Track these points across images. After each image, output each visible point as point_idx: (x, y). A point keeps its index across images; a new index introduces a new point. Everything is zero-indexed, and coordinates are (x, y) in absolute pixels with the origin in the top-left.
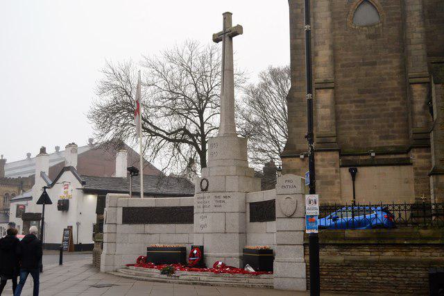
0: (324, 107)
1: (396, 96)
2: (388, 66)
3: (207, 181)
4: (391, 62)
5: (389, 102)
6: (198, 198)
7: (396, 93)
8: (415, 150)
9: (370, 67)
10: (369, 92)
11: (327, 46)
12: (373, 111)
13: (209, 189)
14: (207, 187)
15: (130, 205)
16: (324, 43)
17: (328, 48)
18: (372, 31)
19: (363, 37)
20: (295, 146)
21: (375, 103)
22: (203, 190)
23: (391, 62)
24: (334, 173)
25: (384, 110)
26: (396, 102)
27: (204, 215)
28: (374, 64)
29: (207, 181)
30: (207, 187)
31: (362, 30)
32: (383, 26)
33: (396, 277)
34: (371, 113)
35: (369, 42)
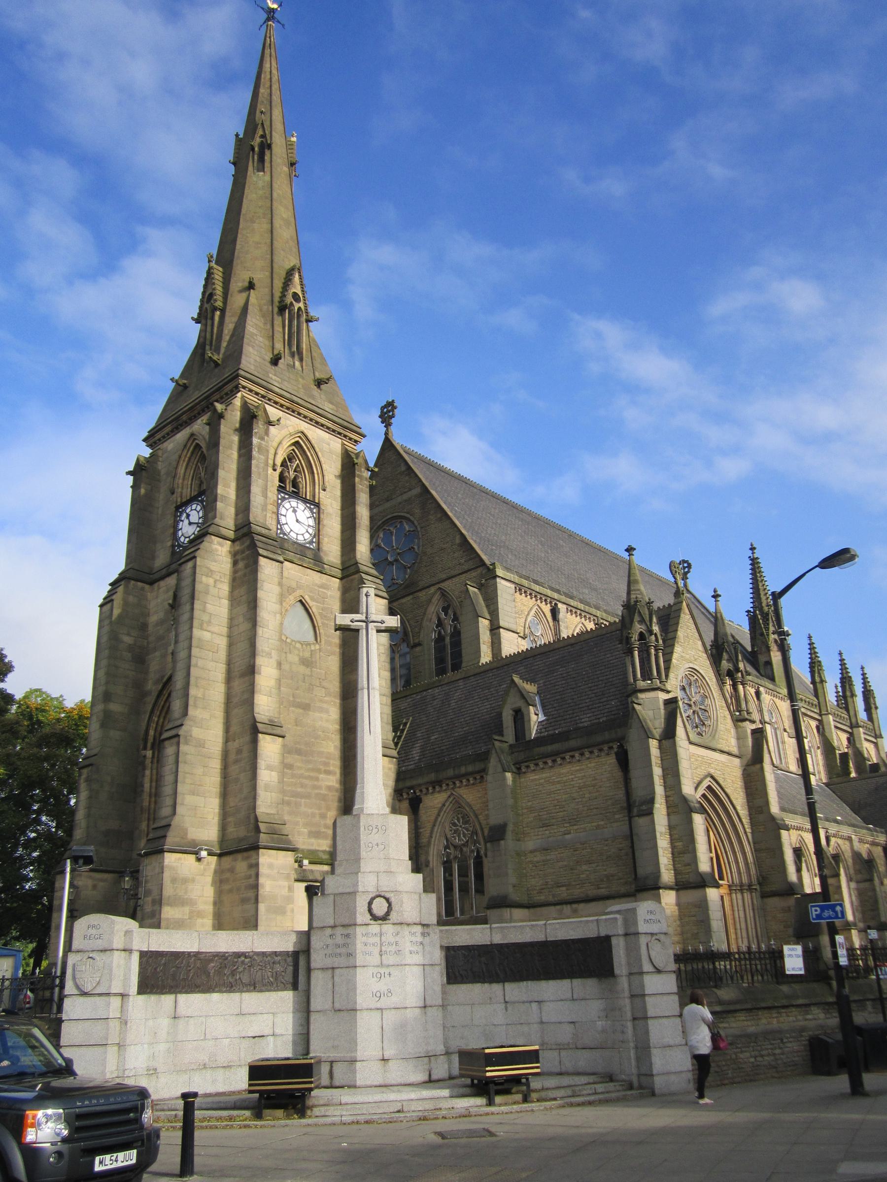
0: (269, 768)
1: (331, 768)
2: (324, 716)
3: (387, 900)
4: (327, 712)
5: (322, 776)
6: (366, 934)
7: (332, 762)
9: (301, 711)
10: (299, 752)
11: (273, 662)
12: (302, 785)
13: (393, 916)
14: (388, 913)
15: (154, 948)
16: (269, 655)
17: (275, 666)
18: (307, 654)
19: (296, 659)
20: (187, 830)
21: (307, 774)
22: (375, 918)
23: (327, 712)
24: (285, 892)
25: (315, 787)
26: (331, 777)
27: (382, 971)
28: (306, 707)
29: (387, 900)
30: (388, 913)
31: (295, 647)
32: (320, 650)
33: (774, 1054)
34: (299, 790)
35: (302, 669)
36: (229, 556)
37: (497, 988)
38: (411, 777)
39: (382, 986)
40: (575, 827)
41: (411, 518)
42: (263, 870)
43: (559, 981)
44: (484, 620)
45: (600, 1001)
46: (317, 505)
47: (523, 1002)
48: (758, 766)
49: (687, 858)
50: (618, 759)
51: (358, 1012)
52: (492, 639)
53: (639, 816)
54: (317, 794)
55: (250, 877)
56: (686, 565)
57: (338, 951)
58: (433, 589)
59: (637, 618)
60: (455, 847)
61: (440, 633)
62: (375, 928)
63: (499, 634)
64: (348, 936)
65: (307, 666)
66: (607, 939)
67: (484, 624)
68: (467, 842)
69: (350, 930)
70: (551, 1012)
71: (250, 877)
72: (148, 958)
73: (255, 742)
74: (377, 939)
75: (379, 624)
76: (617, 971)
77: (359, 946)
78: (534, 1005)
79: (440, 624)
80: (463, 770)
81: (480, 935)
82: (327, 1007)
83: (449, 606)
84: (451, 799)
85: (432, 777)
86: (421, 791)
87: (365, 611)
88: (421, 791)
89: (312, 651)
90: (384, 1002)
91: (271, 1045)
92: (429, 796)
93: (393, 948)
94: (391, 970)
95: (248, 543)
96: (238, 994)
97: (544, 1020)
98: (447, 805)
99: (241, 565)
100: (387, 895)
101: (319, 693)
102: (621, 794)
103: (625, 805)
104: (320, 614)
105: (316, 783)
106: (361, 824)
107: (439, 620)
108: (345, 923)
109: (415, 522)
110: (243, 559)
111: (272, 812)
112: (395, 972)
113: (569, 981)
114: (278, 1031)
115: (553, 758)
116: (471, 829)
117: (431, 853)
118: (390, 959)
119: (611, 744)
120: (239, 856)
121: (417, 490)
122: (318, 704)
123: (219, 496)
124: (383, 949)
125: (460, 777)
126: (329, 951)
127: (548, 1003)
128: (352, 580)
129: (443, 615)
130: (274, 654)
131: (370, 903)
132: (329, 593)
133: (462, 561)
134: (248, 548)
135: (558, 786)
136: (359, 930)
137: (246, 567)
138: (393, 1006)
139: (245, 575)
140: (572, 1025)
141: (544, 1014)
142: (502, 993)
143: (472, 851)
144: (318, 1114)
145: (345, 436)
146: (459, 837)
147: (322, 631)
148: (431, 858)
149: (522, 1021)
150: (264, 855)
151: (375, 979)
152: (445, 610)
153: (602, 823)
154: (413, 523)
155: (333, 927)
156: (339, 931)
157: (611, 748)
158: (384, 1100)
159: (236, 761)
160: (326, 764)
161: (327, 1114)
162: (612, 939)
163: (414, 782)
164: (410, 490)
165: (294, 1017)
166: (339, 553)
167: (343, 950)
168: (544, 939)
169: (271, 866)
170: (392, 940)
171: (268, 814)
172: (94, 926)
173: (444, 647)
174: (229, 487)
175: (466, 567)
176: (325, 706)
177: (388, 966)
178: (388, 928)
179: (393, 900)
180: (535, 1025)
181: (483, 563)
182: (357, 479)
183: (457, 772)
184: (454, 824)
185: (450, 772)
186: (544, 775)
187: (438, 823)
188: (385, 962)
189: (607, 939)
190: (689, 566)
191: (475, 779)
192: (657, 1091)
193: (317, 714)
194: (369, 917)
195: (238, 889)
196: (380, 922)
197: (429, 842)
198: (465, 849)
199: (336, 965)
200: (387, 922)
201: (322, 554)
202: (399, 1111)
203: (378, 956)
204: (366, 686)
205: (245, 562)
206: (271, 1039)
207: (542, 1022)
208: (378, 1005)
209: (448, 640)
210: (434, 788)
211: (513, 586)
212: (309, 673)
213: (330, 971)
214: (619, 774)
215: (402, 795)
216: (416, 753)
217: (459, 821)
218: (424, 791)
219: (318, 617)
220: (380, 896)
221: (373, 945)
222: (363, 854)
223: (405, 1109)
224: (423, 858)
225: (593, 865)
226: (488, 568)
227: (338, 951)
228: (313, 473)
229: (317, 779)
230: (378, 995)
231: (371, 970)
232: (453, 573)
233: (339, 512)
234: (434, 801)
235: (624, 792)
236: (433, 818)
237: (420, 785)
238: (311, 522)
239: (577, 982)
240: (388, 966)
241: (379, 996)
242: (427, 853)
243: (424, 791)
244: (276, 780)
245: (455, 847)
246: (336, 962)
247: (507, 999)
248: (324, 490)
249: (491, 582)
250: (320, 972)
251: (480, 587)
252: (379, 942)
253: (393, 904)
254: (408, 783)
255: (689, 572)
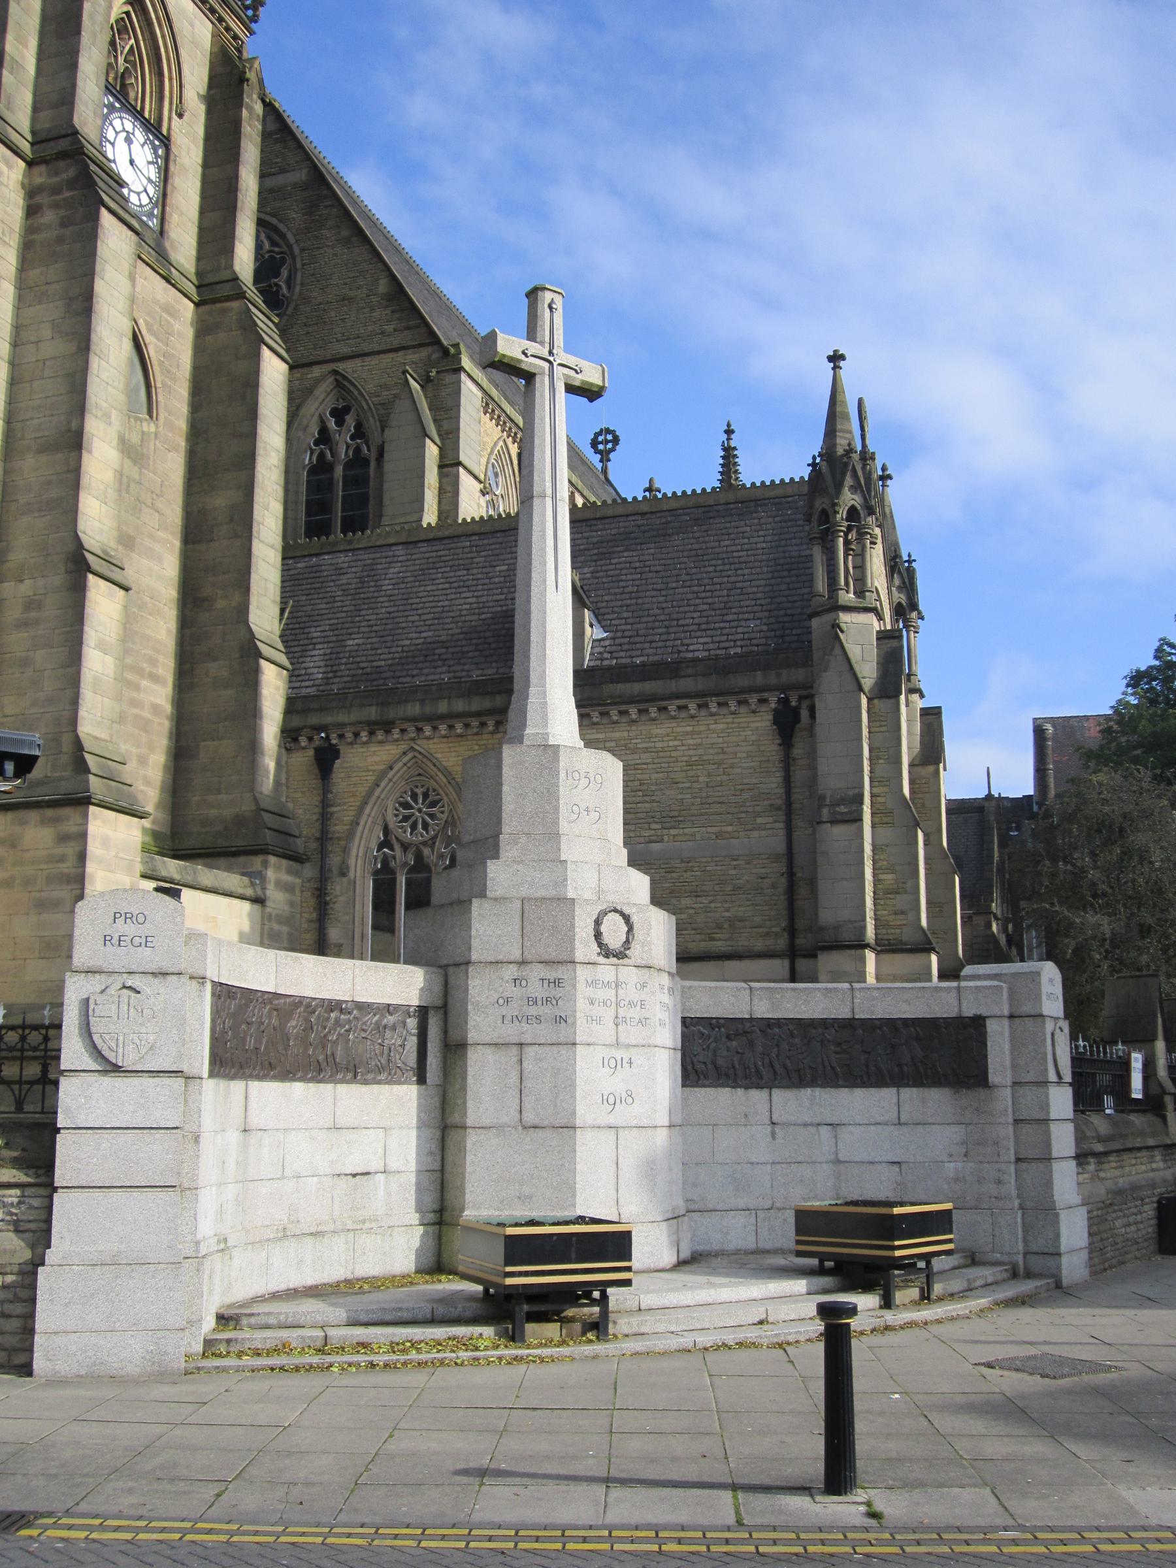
0: (102, 647)
1: (160, 671)
3: (627, 918)
4: (160, 559)
5: (145, 683)
6: (593, 983)
7: (161, 659)
8: (272, 859)
13: (635, 951)
16: (107, 417)
17: (115, 442)
22: (606, 952)
26: (158, 688)
27: (619, 1054)
29: (627, 918)
36: (22, 193)
37: (758, 1096)
38: (321, 710)
39: (614, 1084)
40: (673, 832)
41: (281, 226)
42: (94, 848)
43: (872, 1090)
44: (432, 445)
45: (955, 1128)
46: (166, 142)
47: (805, 1125)
48: (931, 768)
49: (900, 901)
50: (776, 721)
51: (578, 1131)
52: (440, 483)
53: (833, 822)
54: (136, 717)
55: (62, 859)
56: (610, 437)
57: (533, 1011)
58: (316, 372)
59: (849, 481)
60: (405, 847)
61: (322, 456)
62: (607, 971)
63: (457, 476)
64: (557, 982)
65: (135, 462)
66: (978, 1023)
67: (432, 451)
68: (434, 838)
69: (560, 972)
70: (857, 1143)
71: (62, 859)
72: (231, 1001)
73: (78, 591)
74: (610, 994)
75: (572, 373)
76: (993, 1078)
77: (581, 1004)
78: (824, 1130)
79: (324, 437)
80: (443, 707)
81: (733, 999)
82: (505, 1119)
83: (347, 410)
84: (405, 759)
85: (372, 712)
86: (341, 736)
87: (547, 339)
88: (341, 736)
89: (143, 433)
90: (623, 1115)
91: (381, 1192)
92: (358, 749)
93: (635, 1013)
94: (633, 1051)
95: (71, 173)
96: (330, 1086)
97: (842, 1157)
98: (396, 768)
99: (49, 217)
100: (627, 911)
101: (151, 520)
102: (773, 783)
103: (779, 802)
104: (161, 363)
105: (135, 695)
106: (562, 764)
107: (324, 432)
108: (546, 957)
109: (290, 236)
110: (55, 206)
111: (103, 736)
112: (639, 1057)
113: (893, 1090)
114: (393, 1165)
115: (643, 706)
116: (444, 817)
117: (354, 852)
118: (631, 1034)
119: (765, 695)
120: (33, 815)
121: (300, 175)
122: (147, 542)
123: (7, 58)
124: (621, 1013)
125: (433, 719)
126: (508, 1011)
127: (851, 1128)
128: (224, 311)
129: (332, 424)
130: (115, 415)
131: (598, 923)
132: (177, 326)
133: (389, 328)
134: (71, 184)
135: (646, 758)
136: (582, 973)
137: (64, 223)
138: (635, 1123)
139: (60, 240)
140: (896, 1168)
141: (841, 1145)
142: (767, 1106)
143: (441, 856)
144: (626, 1330)
145: (221, 20)
146: (414, 827)
147: (160, 398)
148: (352, 862)
149: (799, 1159)
150: (95, 818)
151: (607, 1069)
152: (339, 415)
153: (729, 829)
154: (283, 236)
155: (523, 963)
156: (536, 973)
157: (763, 701)
158: (710, 1301)
159: (24, 624)
160: (153, 662)
161: (643, 1330)
162: (988, 1022)
163: (329, 719)
164: (283, 171)
165: (419, 1137)
166: (194, 253)
167: (545, 1010)
168: (849, 1016)
169: (106, 842)
170: (635, 996)
171: (96, 738)
172: (128, 917)
173: (331, 483)
174: (26, 46)
175: (395, 341)
176: (157, 547)
177: (628, 1046)
178: (628, 974)
179: (634, 919)
180: (825, 1166)
181: (436, 341)
182: (245, 113)
183: (428, 709)
184: (406, 806)
185: (414, 709)
186: (617, 735)
187: (373, 799)
188: (622, 1039)
189: (978, 1023)
190: (616, 440)
191: (467, 726)
192: (1065, 1282)
193: (145, 562)
194: (595, 947)
195: (28, 882)
196: (614, 960)
197: (351, 835)
198: (426, 851)
199: (527, 1038)
200: (625, 961)
201: (167, 245)
202: (761, 1322)
203: (612, 1025)
204: (549, 491)
205: (62, 212)
206: (380, 1178)
207: (838, 1161)
208: (611, 1120)
209: (339, 471)
210: (372, 733)
211: (479, 394)
212: (137, 477)
213: (515, 1050)
214: (771, 747)
215: (295, 740)
216: (315, 665)
217: (414, 796)
218: (349, 736)
219: (156, 368)
220: (615, 910)
221: (605, 1003)
222: (564, 827)
223: (771, 1319)
224: (334, 860)
225: (704, 900)
226: (446, 352)
227: (533, 1011)
228: (160, 74)
229: (137, 688)
230: (611, 1101)
231: (599, 1053)
232: (366, 347)
233: (200, 169)
234: (368, 762)
235: (780, 780)
236: (362, 790)
237: (343, 725)
238: (153, 173)
239: (908, 1093)
240: (628, 1046)
241: (611, 1101)
242: (345, 850)
243: (349, 736)
244: (112, 675)
245: (405, 847)
246: (528, 1032)
247: (775, 1118)
248: (180, 116)
249: (449, 378)
250: (489, 1051)
251: (426, 382)
252: (614, 1000)
253: (635, 927)
254: (315, 720)
255: (613, 450)
